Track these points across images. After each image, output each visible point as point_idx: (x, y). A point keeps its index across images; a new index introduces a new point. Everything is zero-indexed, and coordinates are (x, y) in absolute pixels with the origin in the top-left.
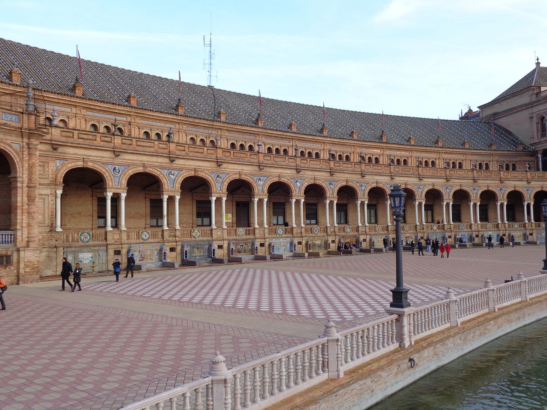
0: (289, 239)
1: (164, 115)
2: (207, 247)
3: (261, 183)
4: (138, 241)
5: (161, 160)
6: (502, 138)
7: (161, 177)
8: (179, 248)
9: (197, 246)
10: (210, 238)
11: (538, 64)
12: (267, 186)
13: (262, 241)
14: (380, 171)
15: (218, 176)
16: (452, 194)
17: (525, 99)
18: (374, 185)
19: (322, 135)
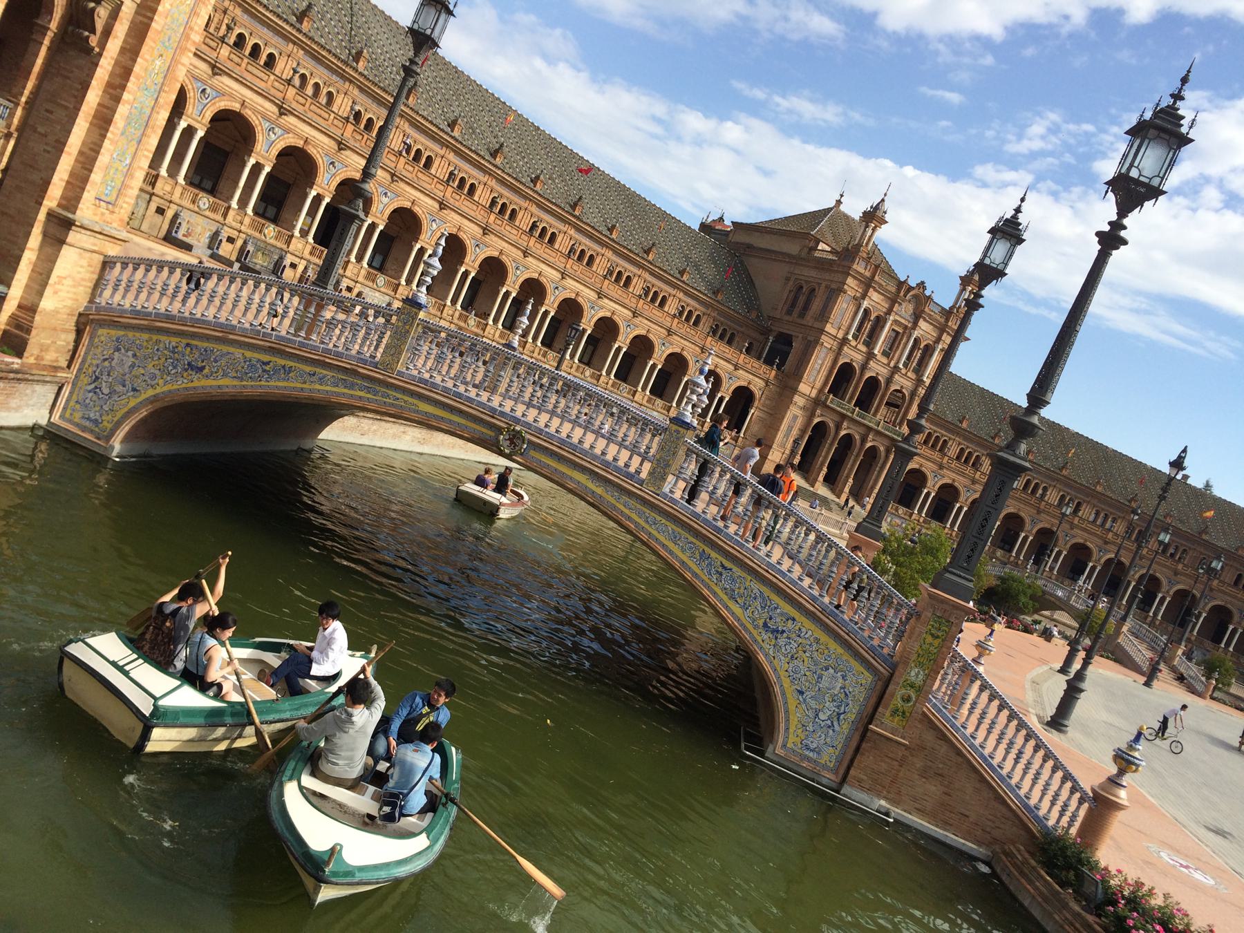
0: (387, 299)
1: (280, 22)
2: (276, 257)
3: (385, 200)
4: (191, 206)
5: (268, 105)
6: (739, 288)
7: (258, 129)
8: (239, 243)
9: (264, 249)
10: (285, 247)
11: (839, 202)
12: (391, 208)
13: (351, 284)
14: (551, 259)
15: (332, 163)
16: (631, 336)
17: (793, 248)
18: (535, 276)
19: (492, 160)
